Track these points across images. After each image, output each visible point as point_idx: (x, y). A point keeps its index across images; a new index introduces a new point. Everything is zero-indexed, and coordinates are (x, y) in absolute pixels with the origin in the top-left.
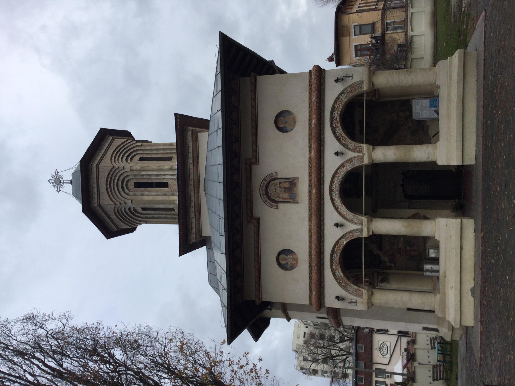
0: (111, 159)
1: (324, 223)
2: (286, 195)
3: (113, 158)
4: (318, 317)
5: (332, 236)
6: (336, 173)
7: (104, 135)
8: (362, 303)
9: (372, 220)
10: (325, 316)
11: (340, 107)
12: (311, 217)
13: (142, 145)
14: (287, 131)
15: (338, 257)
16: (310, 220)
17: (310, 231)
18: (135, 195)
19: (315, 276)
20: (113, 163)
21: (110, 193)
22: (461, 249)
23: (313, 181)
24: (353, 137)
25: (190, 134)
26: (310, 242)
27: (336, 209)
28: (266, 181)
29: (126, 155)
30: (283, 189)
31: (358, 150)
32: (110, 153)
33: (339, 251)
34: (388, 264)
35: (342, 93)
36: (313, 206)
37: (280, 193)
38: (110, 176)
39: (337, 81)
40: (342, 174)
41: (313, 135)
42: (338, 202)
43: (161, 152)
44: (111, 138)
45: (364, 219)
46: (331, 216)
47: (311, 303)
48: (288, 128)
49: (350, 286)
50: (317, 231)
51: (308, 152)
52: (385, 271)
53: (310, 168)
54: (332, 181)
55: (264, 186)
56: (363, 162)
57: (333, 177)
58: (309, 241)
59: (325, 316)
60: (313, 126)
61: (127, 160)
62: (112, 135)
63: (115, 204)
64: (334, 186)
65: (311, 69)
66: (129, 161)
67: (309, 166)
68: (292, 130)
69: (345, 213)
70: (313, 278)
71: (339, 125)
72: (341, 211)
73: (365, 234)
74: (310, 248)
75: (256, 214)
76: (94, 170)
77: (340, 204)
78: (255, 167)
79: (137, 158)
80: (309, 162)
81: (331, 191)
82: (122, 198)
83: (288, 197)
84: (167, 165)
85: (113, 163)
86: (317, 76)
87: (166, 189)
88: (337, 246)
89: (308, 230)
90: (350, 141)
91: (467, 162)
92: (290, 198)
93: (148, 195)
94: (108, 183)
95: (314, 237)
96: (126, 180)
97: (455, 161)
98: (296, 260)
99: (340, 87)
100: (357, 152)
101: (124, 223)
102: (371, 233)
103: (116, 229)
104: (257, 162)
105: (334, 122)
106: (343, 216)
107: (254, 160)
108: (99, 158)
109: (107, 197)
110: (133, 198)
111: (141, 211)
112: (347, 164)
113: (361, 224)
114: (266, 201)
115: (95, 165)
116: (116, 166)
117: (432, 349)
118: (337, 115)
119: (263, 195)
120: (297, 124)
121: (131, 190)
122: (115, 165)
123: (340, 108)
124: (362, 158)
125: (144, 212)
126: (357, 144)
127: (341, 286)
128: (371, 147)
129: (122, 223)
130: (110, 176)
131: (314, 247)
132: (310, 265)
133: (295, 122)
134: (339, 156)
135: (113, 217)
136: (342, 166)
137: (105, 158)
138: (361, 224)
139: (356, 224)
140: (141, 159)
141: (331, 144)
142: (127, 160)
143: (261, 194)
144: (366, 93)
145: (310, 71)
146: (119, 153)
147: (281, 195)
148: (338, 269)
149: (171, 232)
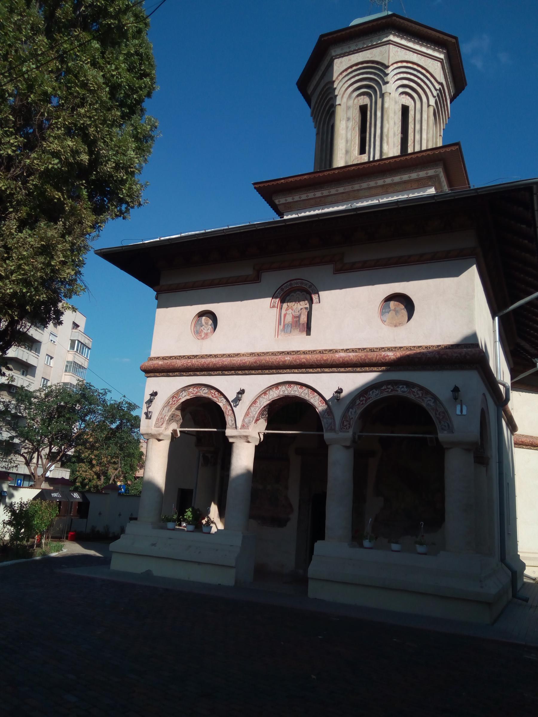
2: (289, 319)
3: (400, 65)
5: (227, 385)
8: (148, 426)
11: (414, 396)
13: (429, 106)
15: (204, 395)
16: (252, 354)
17: (237, 355)
18: (348, 108)
19: (179, 363)
20: (396, 66)
21: (350, 70)
23: (302, 356)
25: (431, 172)
26: (223, 355)
27: (265, 393)
29: (412, 84)
30: (297, 314)
31: (345, 424)
32: (415, 58)
33: (210, 397)
35: (435, 398)
36: (267, 358)
37: (292, 310)
39: (456, 390)
42: (274, 395)
43: (418, 137)
44: (442, 56)
47: (151, 359)
48: (388, 317)
49: (168, 411)
51: (345, 348)
53: (321, 352)
54: (302, 385)
55: (303, 286)
58: (224, 355)
62: (449, 56)
66: (401, 90)
67: (326, 350)
68: (383, 321)
69: (258, 404)
70: (178, 361)
71: (385, 394)
72: (261, 399)
73: (229, 432)
74: (216, 356)
75: (266, 277)
77: (271, 397)
78: (330, 268)
80: (331, 350)
83: (286, 322)
85: (396, 66)
88: (216, 393)
90: (359, 411)
91: (311, 585)
93: (347, 127)
95: (227, 361)
103: (309, 92)
104: (337, 271)
105: (389, 386)
108: (404, 42)
109: (345, 67)
114: (282, 290)
115: (391, 38)
118: (401, 391)
119: (291, 285)
121: (356, 100)
123: (412, 397)
124: (332, 429)
132: (195, 356)
133: (395, 326)
137: (404, 51)
138: (243, 426)
140: (405, 110)
143: (292, 282)
147: (290, 311)
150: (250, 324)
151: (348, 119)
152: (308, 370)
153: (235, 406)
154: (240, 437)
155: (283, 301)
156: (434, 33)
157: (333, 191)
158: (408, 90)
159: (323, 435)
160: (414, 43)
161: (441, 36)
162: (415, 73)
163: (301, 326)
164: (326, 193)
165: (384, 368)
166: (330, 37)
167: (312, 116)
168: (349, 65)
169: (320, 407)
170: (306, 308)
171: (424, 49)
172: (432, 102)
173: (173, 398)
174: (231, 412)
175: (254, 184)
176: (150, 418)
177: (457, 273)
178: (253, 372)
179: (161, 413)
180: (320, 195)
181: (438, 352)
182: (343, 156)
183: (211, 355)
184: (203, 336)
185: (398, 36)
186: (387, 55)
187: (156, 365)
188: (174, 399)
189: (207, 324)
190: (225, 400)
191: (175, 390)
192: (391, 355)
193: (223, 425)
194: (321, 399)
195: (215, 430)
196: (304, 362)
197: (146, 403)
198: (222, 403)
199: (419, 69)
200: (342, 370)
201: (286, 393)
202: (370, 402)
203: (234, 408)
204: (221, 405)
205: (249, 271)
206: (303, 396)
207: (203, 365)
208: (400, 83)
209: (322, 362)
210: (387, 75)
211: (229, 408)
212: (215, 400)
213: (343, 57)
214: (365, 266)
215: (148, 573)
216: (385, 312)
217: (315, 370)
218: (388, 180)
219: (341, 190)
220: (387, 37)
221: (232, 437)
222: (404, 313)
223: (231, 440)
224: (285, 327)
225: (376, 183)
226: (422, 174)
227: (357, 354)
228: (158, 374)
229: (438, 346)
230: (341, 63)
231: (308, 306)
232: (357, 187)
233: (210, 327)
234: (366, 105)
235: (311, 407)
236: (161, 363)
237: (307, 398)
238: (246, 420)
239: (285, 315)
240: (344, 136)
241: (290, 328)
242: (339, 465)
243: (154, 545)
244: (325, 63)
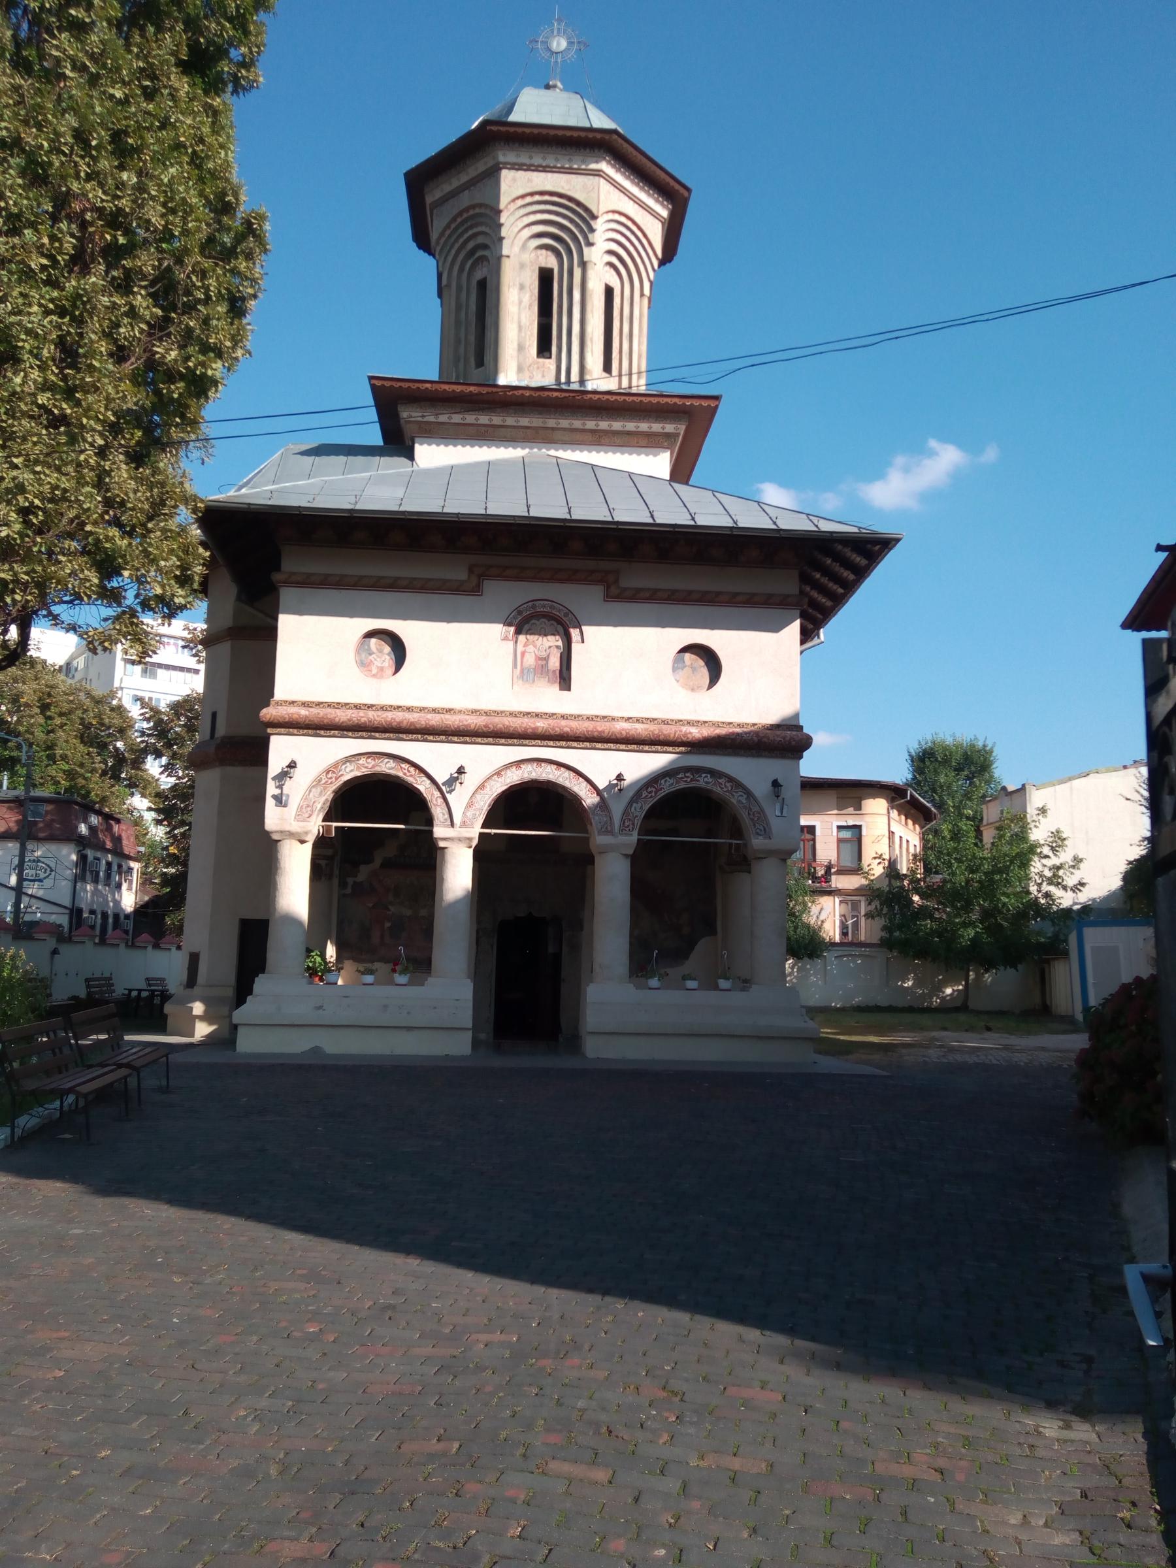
0: (614, 212)
2: (530, 660)
4: (214, 715)
5: (437, 758)
10: (221, 731)
11: (719, 789)
12: (481, 714)
13: (642, 295)
14: (674, 669)
15: (388, 771)
16: (474, 712)
17: (449, 711)
18: (522, 266)
19: (342, 716)
22: (409, 1028)
23: (563, 723)
24: (651, 814)
25: (670, 428)
26: (422, 709)
27: (498, 773)
28: (566, 615)
30: (544, 654)
33: (400, 774)
34: (350, 881)
35: (748, 793)
39: (776, 784)
41: (664, 727)
42: (514, 777)
49: (320, 794)
51: (626, 715)
52: (336, 872)
54: (560, 765)
56: (600, 833)
58: (424, 708)
59: (221, 731)
60: (684, 729)
61: (611, 252)
62: (672, 214)
65: (805, 731)
69: (487, 790)
71: (682, 785)
72: (492, 782)
73: (439, 831)
75: (489, 586)
77: (508, 781)
78: (598, 591)
79: (615, 282)
80: (604, 717)
82: (516, 230)
83: (526, 664)
84: (595, 359)
86: (790, 742)
87: (534, 350)
88: (412, 769)
89: (451, 706)
90: (646, 807)
92: (522, 670)
93: (520, 302)
95: (434, 720)
97: (592, 1019)
99: (761, 789)
100: (623, 822)
101: (448, 226)
103: (429, 199)
104: (609, 597)
107: (614, 591)
109: (521, 192)
111: (479, 275)
115: (604, 166)
116: (600, 225)
117: (87, 980)
118: (703, 782)
119: (534, 607)
120: (689, 692)
122: (600, 221)
123: (718, 789)
124: (608, 831)
125: (474, 283)
126: (638, 822)
129: (447, 221)
133: (693, 690)
135: (465, 200)
138: (464, 824)
140: (609, 291)
142: (611, 252)
143: (537, 603)
144: (745, 845)
145: (801, 728)
146: (628, 233)
147: (531, 648)
148: (358, 769)
150: (464, 661)
151: (522, 287)
152: (570, 743)
153: (450, 792)
154: (460, 839)
155: (518, 632)
156: (663, 175)
157: (510, 421)
160: (633, 182)
161: (672, 183)
162: (628, 233)
163: (551, 674)
164: (497, 420)
165: (682, 749)
166: (501, 128)
167: (422, 238)
168: (529, 190)
169: (590, 800)
170: (557, 647)
171: (643, 196)
173: (328, 773)
174: (440, 800)
175: (371, 378)
176: (285, 806)
177: (776, 628)
178: (479, 740)
179: (305, 798)
180: (487, 422)
181: (756, 733)
182: (515, 353)
183: (399, 707)
184: (374, 671)
185: (613, 166)
186: (595, 196)
187: (295, 716)
188: (330, 775)
189: (380, 651)
190: (428, 782)
191: (331, 760)
192: (696, 733)
193: (430, 821)
194: (589, 787)
195: (402, 826)
196: (567, 733)
197: (274, 779)
198: (423, 785)
200: (623, 747)
201: (534, 776)
202: (661, 794)
203: (448, 796)
204: (421, 788)
205: (458, 573)
206: (560, 781)
207: (391, 723)
209: (596, 734)
210: (592, 230)
211: (437, 794)
212: (410, 780)
213: (517, 170)
214: (653, 596)
215: (316, 1050)
216: (678, 668)
217: (582, 745)
218: (604, 425)
219: (524, 421)
220: (597, 162)
222: (704, 673)
223: (441, 844)
224: (526, 674)
225: (584, 424)
226: (657, 427)
227: (645, 726)
228: (295, 731)
229: (754, 725)
230: (514, 180)
231: (560, 643)
232: (551, 423)
233: (388, 658)
234: (551, 271)
235: (575, 800)
236: (304, 712)
237: (567, 784)
238: (469, 814)
239: (523, 654)
240: (516, 317)
241: (531, 676)
242: (612, 882)
243: (320, 1008)
244: (481, 166)
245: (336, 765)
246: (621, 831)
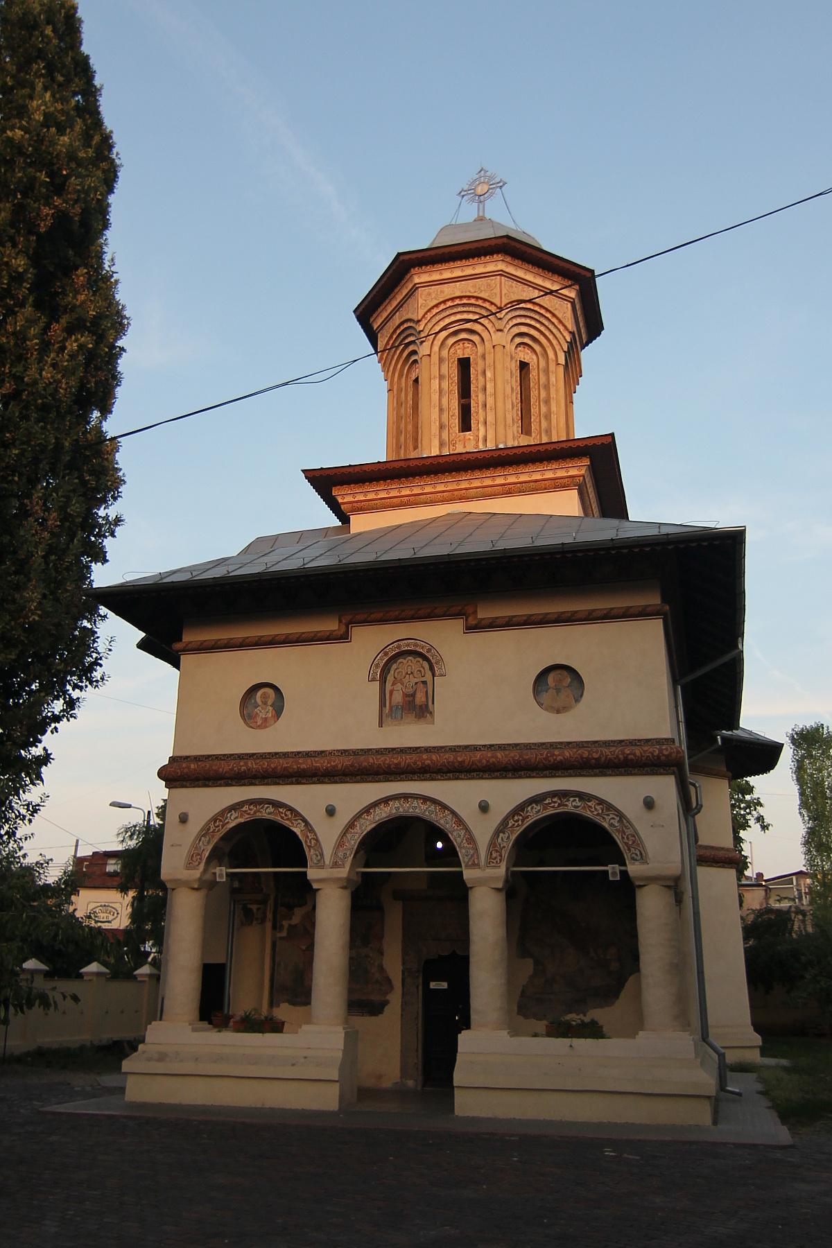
1: (336, 782)
5: (306, 800)
6: (444, 807)
7: (582, 281)
9: (344, 888)
27: (367, 810)
38: (480, 302)
40: (442, 822)
42: (383, 813)
45: (343, 872)
46: (352, 798)
50: (317, 769)
54: (425, 799)
57: (434, 801)
63: (419, 321)
64: (415, 803)
66: (518, 340)
71: (550, 811)
76: (491, 267)
79: (526, 356)
81: (406, 797)
90: (513, 837)
94: (465, 301)
95: (304, 764)
96: (475, 338)
98: (265, 724)
102: (315, 886)
106: (351, 825)
110: (435, 358)
112: (463, 833)
113: (335, 865)
118: (572, 806)
123: (588, 814)
124: (475, 865)
126: (505, 854)
127: (210, 821)
128: (500, 885)
130: (480, 302)
131: (284, 763)
134: (481, 813)
136: (460, 821)
139: (335, 854)
140: (524, 366)
141: (508, 794)
146: (537, 317)
149: (372, 448)
158: (526, 340)
159: (461, 873)
162: (537, 317)
172: (562, 360)
199: (542, 311)
208: (516, 330)
221: (318, 881)
245: (223, 813)
246: (488, 864)
